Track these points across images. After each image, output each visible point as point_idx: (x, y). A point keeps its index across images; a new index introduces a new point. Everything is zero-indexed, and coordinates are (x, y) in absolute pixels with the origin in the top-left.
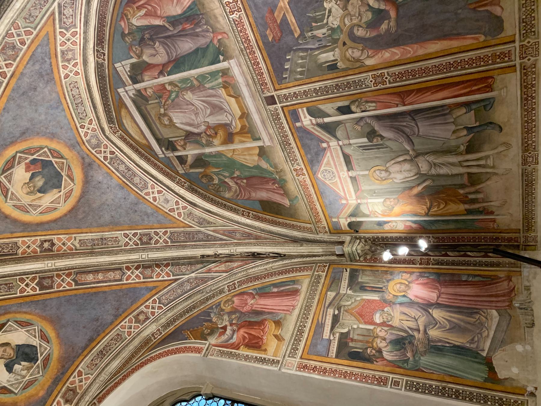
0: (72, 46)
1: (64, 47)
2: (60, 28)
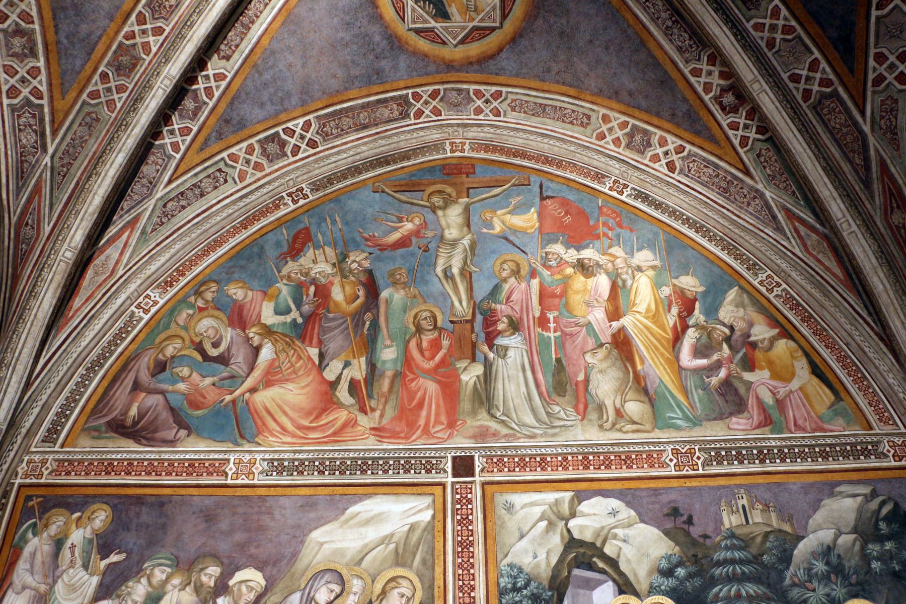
0: (15, 66)
1: (31, 65)
2: (42, 106)
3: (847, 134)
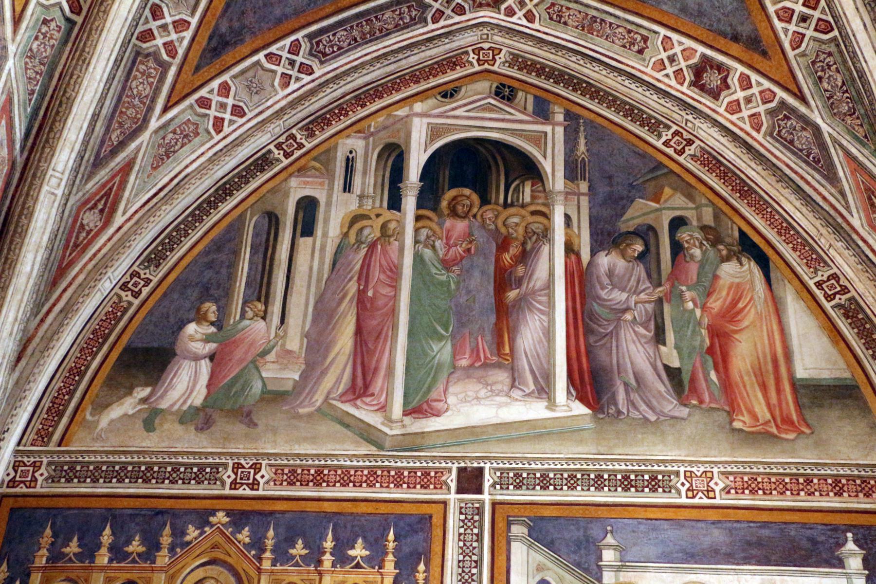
3: (134, 106)
